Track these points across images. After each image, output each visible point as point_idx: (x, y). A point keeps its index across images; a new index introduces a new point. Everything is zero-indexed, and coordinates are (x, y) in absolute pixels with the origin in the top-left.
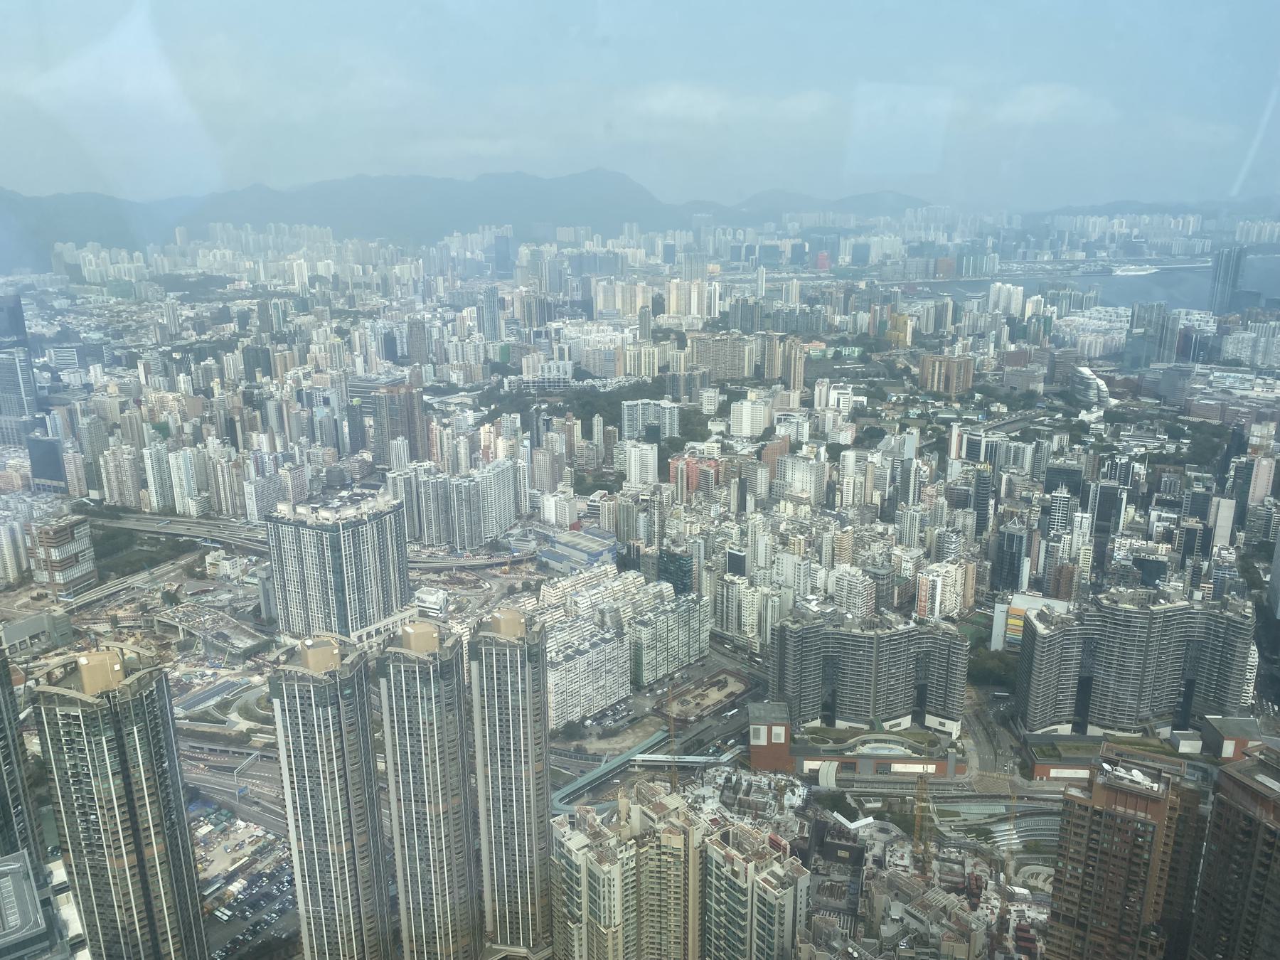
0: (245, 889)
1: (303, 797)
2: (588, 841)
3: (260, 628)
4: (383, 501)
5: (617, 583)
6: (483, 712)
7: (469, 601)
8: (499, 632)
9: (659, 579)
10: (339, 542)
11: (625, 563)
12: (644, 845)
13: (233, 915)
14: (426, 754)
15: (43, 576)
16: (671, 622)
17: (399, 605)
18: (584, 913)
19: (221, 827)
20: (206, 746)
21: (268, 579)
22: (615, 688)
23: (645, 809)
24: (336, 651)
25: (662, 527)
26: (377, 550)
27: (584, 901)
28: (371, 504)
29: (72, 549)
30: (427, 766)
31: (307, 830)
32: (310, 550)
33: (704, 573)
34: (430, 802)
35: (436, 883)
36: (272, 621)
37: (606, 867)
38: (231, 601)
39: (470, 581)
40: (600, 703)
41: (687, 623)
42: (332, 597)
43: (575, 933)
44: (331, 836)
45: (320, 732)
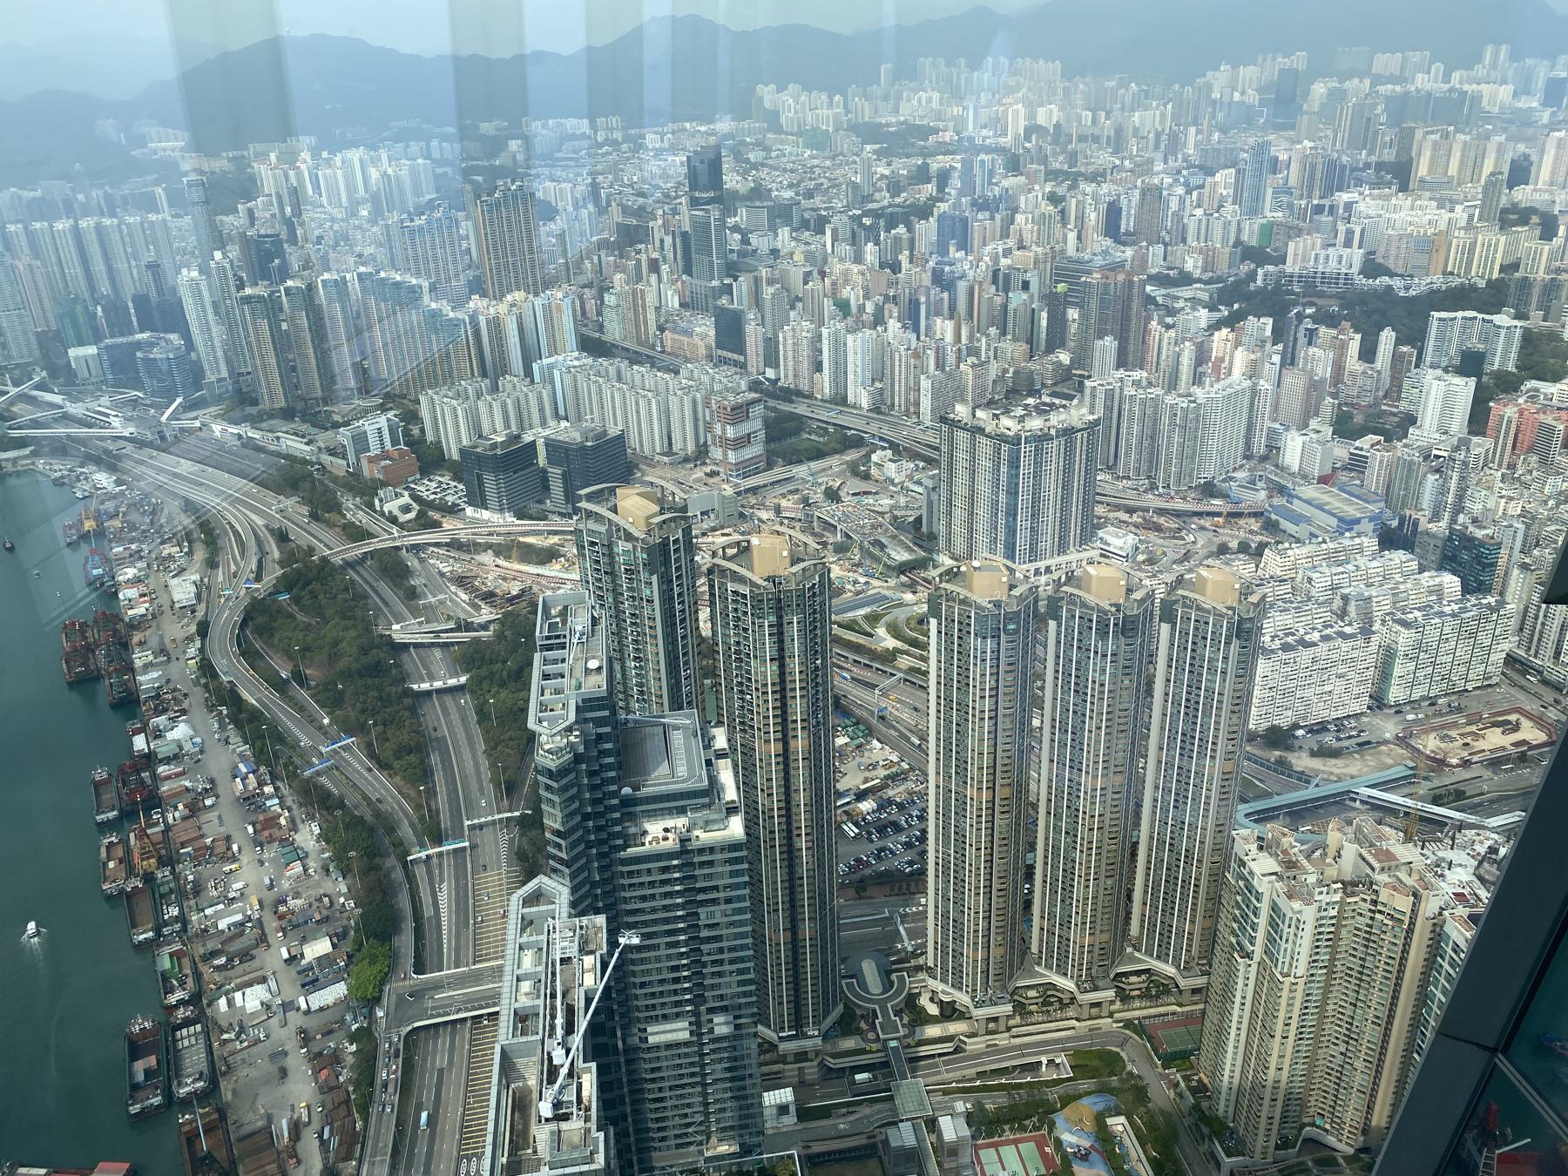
0: (873, 812)
1: (948, 730)
2: (1278, 869)
3: (918, 541)
4: (1077, 414)
5: (1375, 564)
6: (1167, 686)
7: (1164, 554)
8: (1203, 595)
9: (1440, 568)
10: (1018, 458)
11: (1390, 540)
12: (1353, 894)
13: (860, 834)
14: (1091, 718)
15: (716, 453)
16: (1447, 630)
17: (1077, 544)
18: (1258, 950)
19: (857, 742)
20: (851, 656)
21: (934, 489)
22: (1345, 698)
23: (1364, 852)
24: (1004, 579)
25: (1460, 497)
26: (1061, 473)
27: (1260, 936)
28: (1062, 417)
29: (745, 428)
30: (1090, 731)
31: (947, 766)
32: (985, 463)
33: (1516, 572)
34: (1087, 773)
35: (1080, 864)
36: (933, 537)
37: (1297, 905)
38: (892, 507)
39: (1170, 530)
40: (1321, 712)
41: (1473, 635)
42: (1002, 521)
43: (1241, 968)
44: (972, 778)
45: (975, 664)
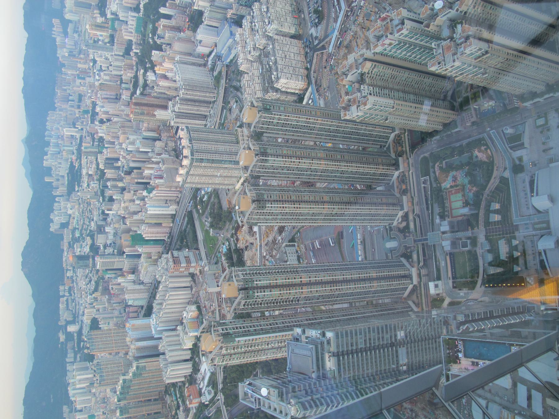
11: (238, 22)
15: (192, 270)
29: (182, 259)
32: (200, 171)
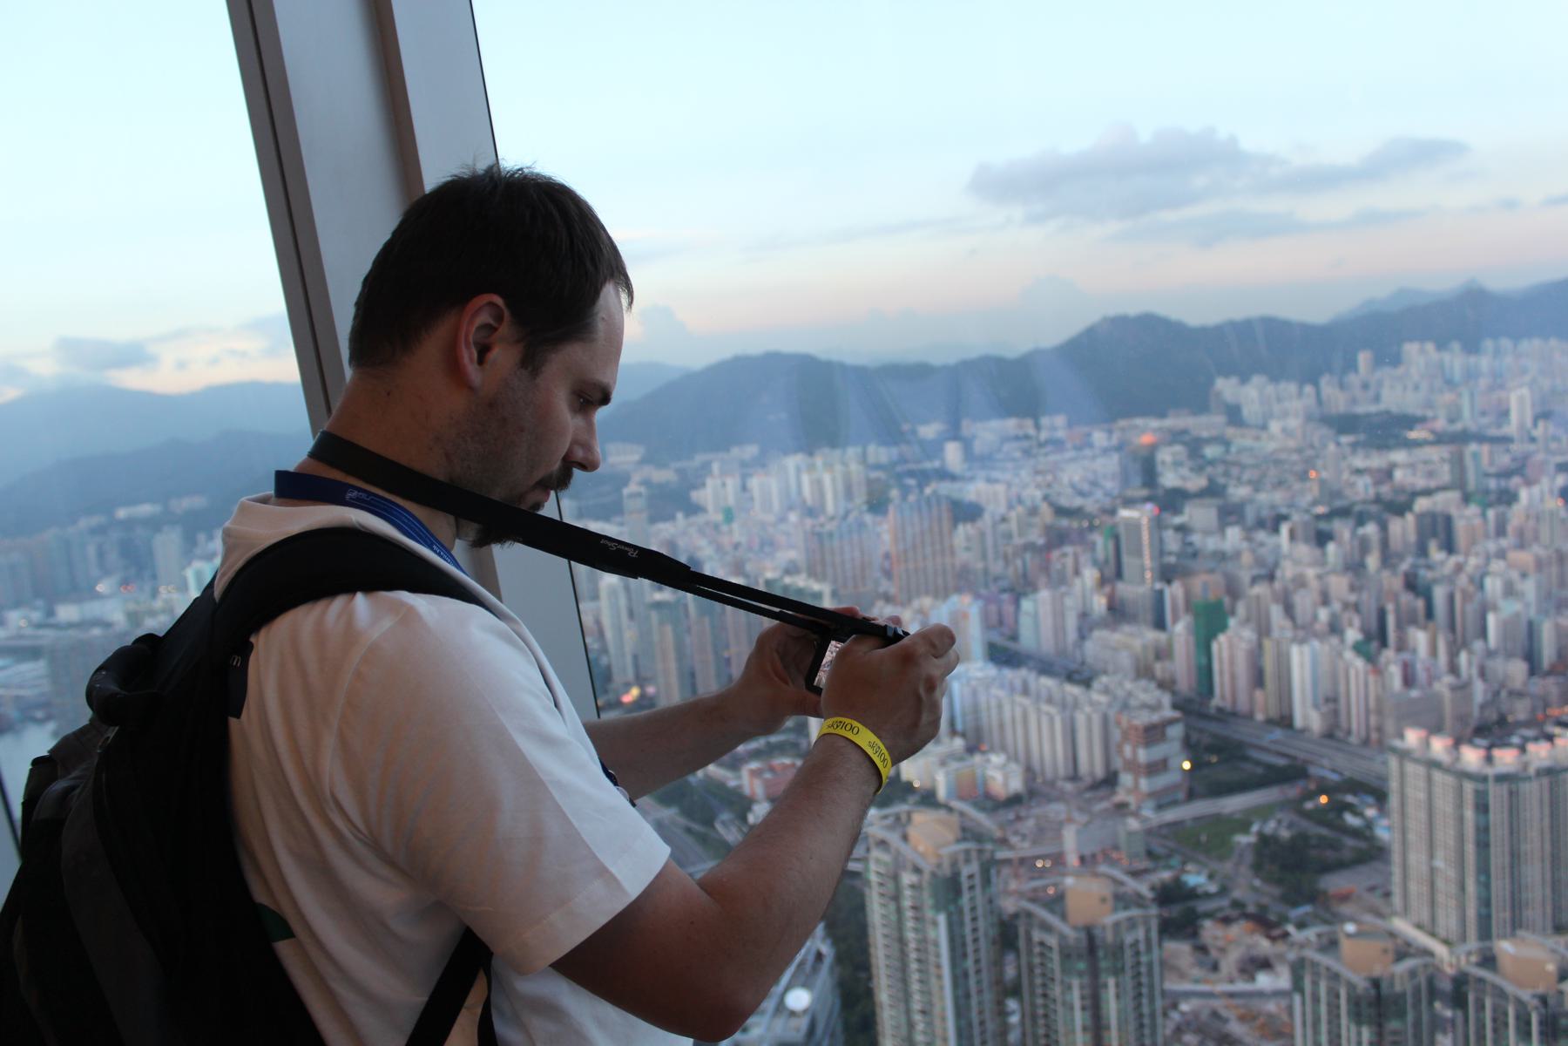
15: (1126, 779)
29: (1158, 752)
32: (1444, 805)
